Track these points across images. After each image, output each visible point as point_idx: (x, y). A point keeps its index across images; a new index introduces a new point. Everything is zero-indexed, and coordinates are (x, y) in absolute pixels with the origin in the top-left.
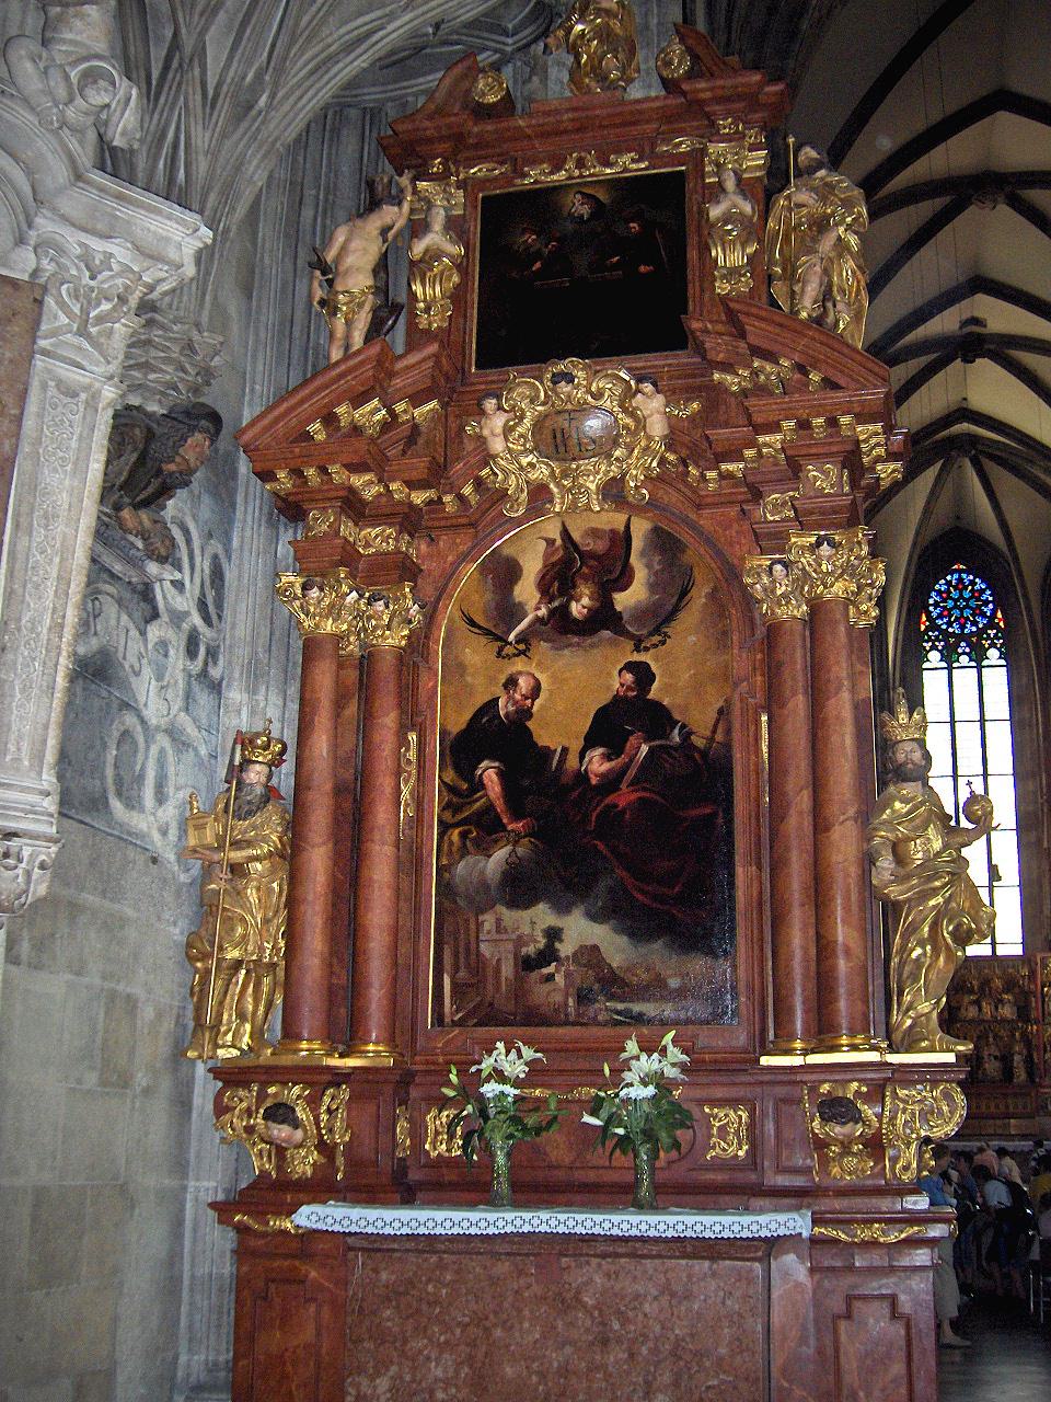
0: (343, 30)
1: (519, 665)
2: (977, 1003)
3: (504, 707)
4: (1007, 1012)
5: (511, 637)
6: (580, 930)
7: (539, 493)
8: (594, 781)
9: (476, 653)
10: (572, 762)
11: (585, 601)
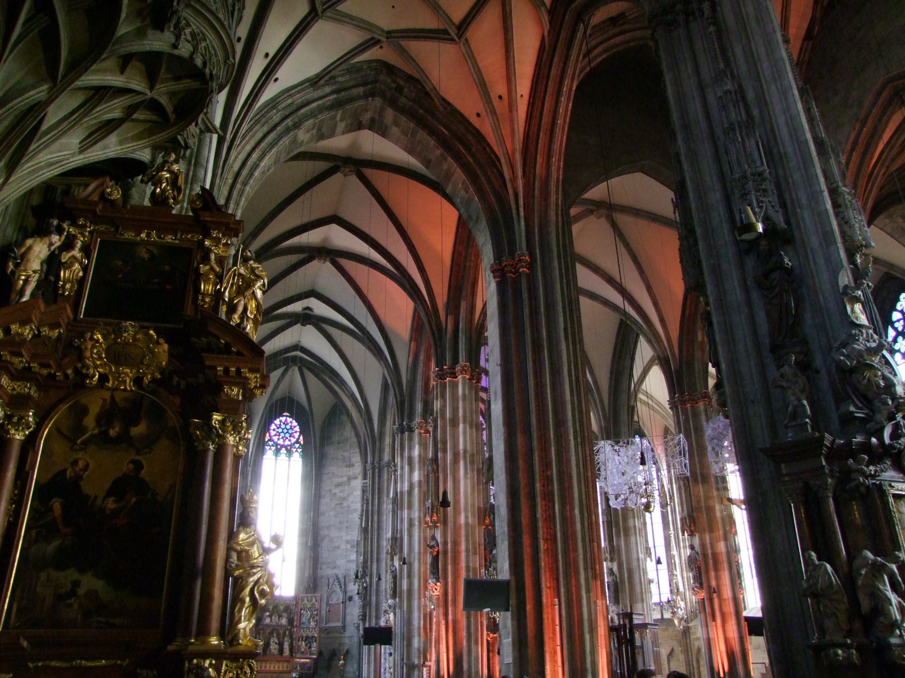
0: (49, 157)
1: (80, 455)
2: (270, 616)
3: (69, 473)
4: (284, 621)
5: (79, 442)
6: (90, 583)
7: (103, 378)
8: (108, 512)
9: (60, 447)
10: (99, 502)
11: (117, 429)
